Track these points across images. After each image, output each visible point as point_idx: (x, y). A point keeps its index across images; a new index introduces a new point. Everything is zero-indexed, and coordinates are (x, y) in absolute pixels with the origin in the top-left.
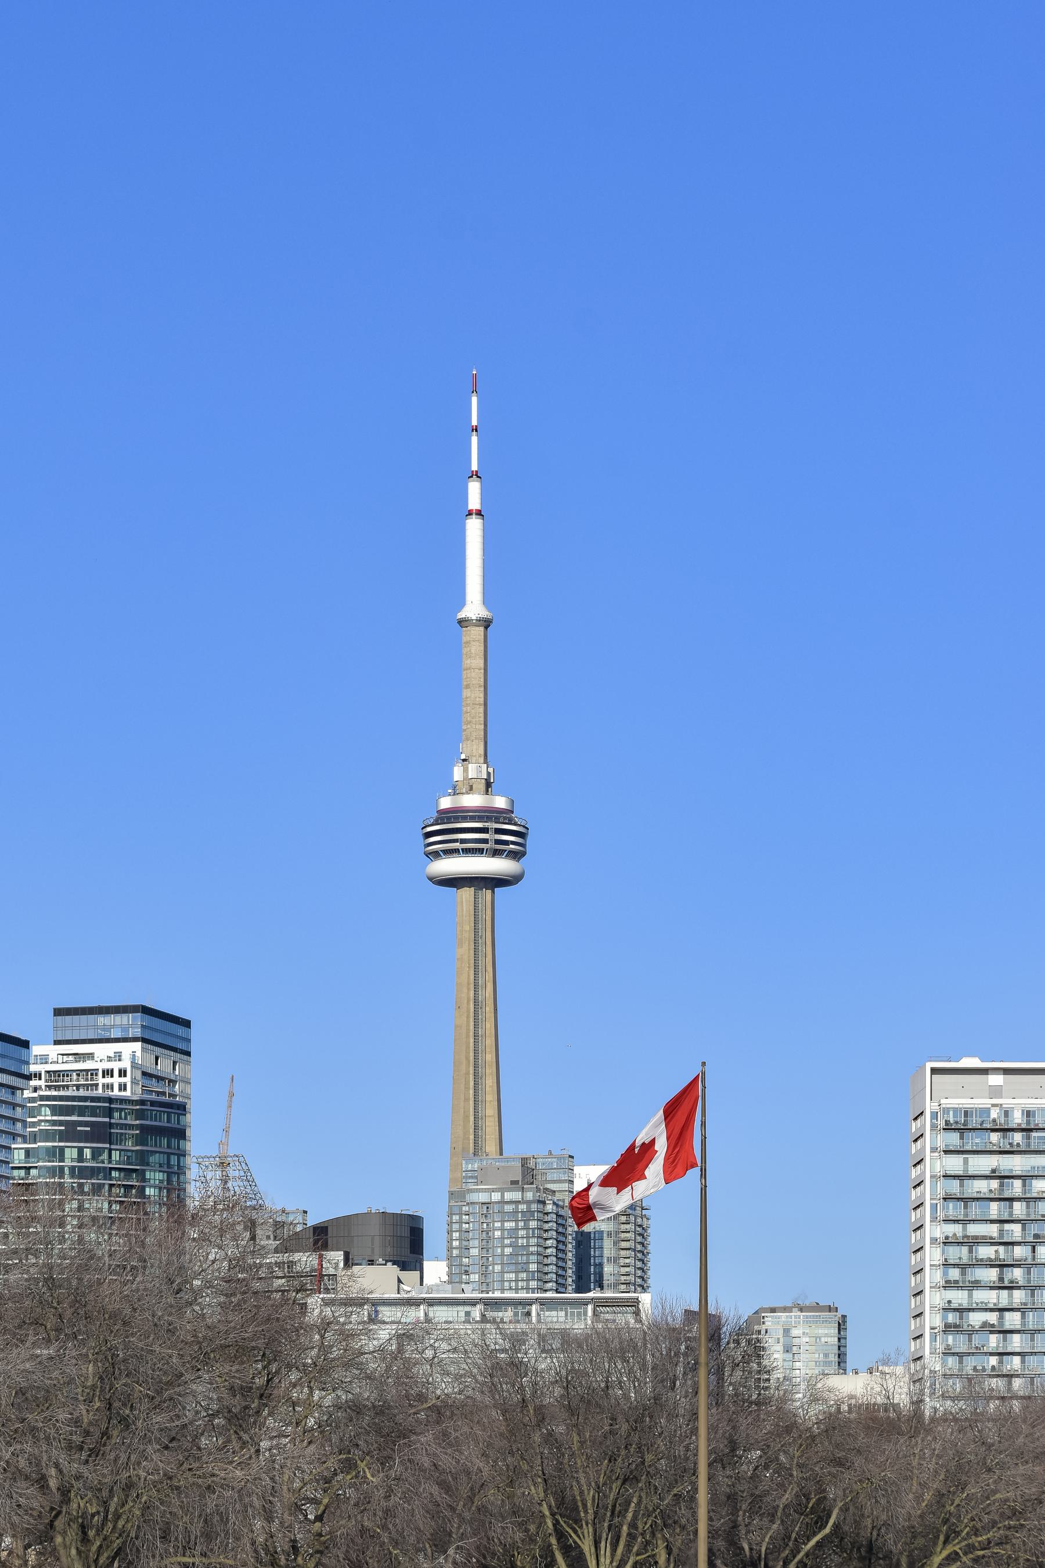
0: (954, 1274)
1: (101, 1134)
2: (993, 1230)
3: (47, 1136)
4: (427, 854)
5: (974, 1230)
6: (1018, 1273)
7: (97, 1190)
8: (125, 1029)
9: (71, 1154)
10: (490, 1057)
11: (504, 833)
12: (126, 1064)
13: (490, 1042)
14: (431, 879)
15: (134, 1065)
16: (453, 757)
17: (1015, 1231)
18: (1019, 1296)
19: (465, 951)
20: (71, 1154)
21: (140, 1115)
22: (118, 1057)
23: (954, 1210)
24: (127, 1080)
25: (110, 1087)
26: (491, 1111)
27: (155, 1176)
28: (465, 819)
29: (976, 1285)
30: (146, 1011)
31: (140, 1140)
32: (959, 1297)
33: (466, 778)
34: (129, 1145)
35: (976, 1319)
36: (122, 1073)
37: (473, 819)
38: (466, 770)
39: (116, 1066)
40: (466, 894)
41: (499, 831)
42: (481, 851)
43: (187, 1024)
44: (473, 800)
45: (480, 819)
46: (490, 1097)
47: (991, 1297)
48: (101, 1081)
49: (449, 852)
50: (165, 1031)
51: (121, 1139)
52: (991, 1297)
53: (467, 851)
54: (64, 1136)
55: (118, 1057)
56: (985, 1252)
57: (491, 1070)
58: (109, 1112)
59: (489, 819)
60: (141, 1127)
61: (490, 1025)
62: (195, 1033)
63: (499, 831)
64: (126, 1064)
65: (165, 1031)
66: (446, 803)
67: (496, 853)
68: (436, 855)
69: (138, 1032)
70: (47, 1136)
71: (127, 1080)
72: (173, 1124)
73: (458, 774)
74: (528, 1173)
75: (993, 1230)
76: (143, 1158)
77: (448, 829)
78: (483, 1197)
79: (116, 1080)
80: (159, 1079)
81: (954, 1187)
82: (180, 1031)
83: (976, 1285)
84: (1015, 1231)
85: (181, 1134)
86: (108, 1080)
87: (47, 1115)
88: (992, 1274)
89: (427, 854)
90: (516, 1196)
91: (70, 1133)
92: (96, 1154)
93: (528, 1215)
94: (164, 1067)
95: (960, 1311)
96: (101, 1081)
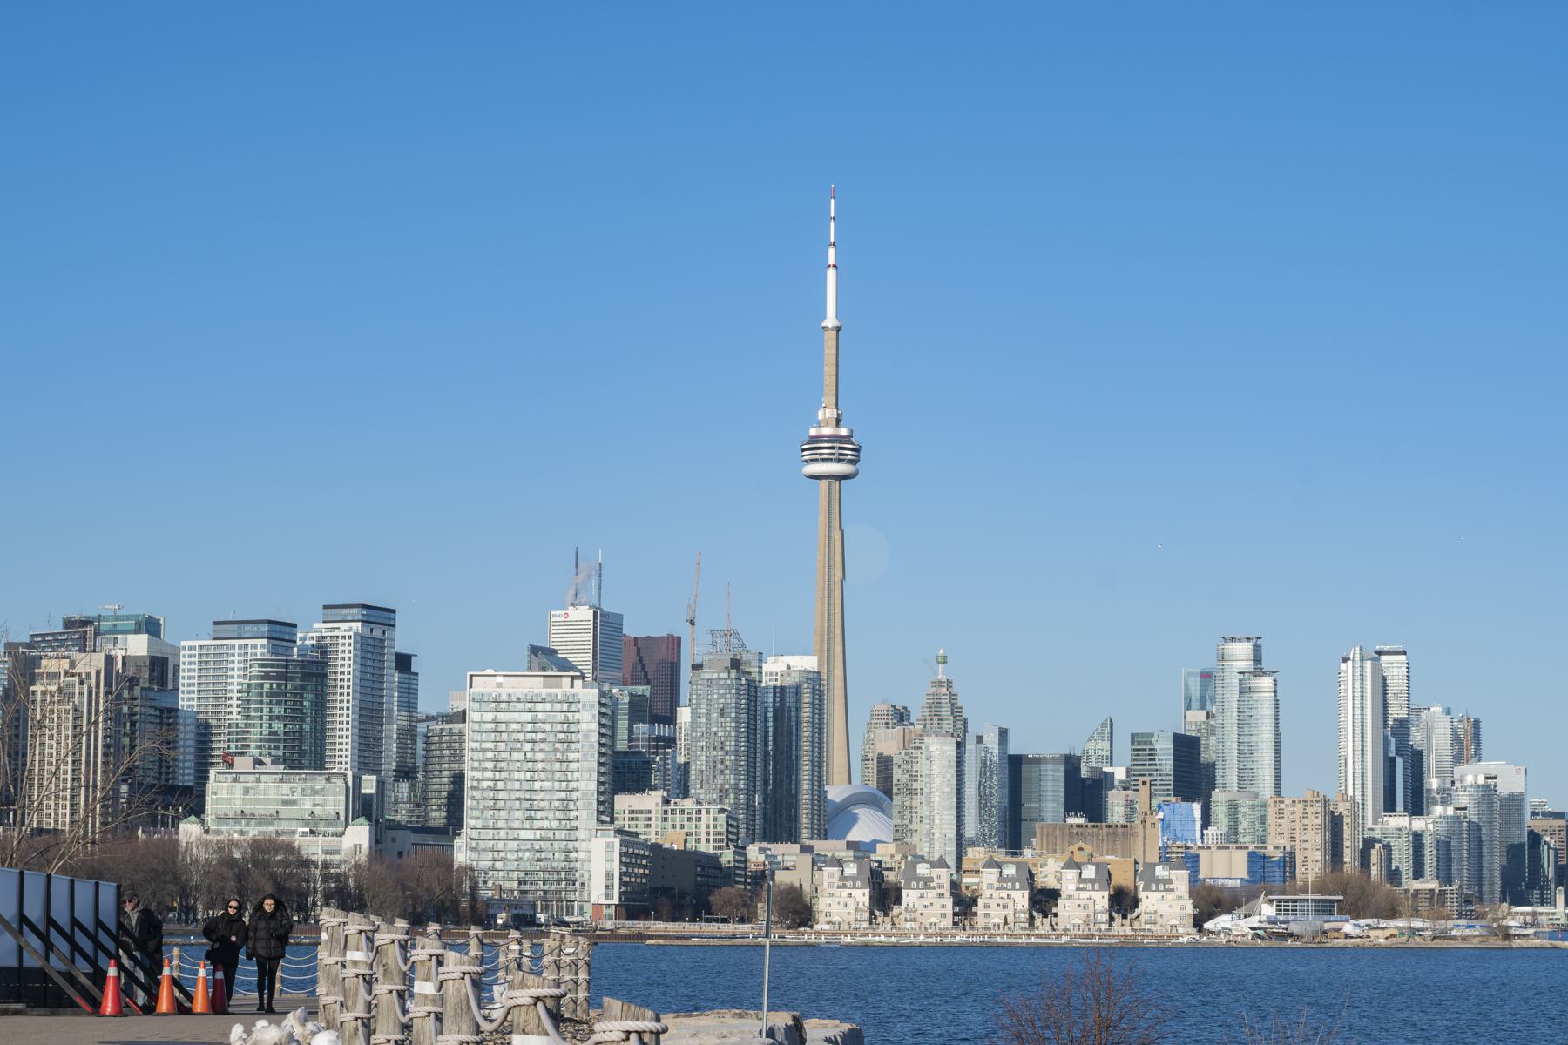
0: (476, 764)
1: (284, 676)
2: (491, 745)
3: (257, 677)
5: (485, 745)
6: (503, 765)
7: (279, 703)
9: (267, 686)
17: (502, 746)
18: (504, 775)
19: (822, 518)
20: (267, 686)
21: (303, 667)
23: (477, 737)
26: (838, 610)
27: (309, 696)
29: (485, 769)
30: (364, 606)
32: (477, 775)
35: (485, 784)
43: (394, 611)
46: (838, 602)
47: (489, 774)
50: (379, 617)
51: (292, 679)
52: (489, 774)
53: (823, 460)
54: (263, 678)
56: (490, 755)
58: (287, 666)
62: (398, 615)
65: (379, 617)
70: (257, 677)
74: (736, 664)
75: (491, 745)
76: (303, 688)
78: (708, 676)
81: (476, 727)
83: (485, 769)
84: (502, 746)
88: (490, 765)
90: (725, 675)
91: (266, 676)
92: (279, 686)
93: (731, 687)
94: (378, 632)
95: (478, 780)
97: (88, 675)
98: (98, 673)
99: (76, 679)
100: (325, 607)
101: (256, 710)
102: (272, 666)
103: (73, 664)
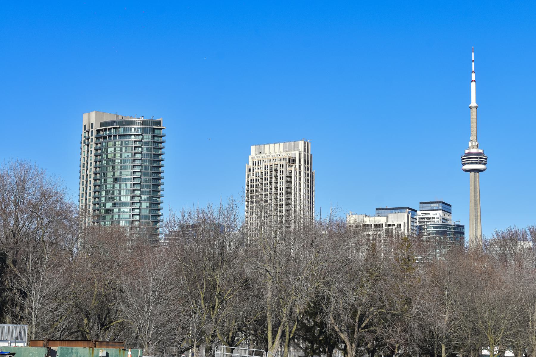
1: (445, 233)
4: (463, 164)
8: (438, 207)
10: (479, 214)
11: (481, 158)
12: (438, 216)
13: (478, 210)
14: (463, 170)
15: (440, 216)
16: (469, 140)
21: (454, 228)
22: (436, 214)
24: (439, 220)
25: (434, 222)
28: (472, 155)
30: (443, 203)
31: (454, 235)
33: (472, 145)
34: (451, 236)
36: (437, 218)
37: (474, 155)
38: (472, 143)
39: (436, 216)
40: (472, 174)
41: (480, 158)
42: (476, 163)
43: (450, 206)
44: (474, 151)
45: (476, 155)
48: (432, 220)
49: (468, 163)
53: (472, 163)
55: (436, 214)
57: (479, 217)
58: (447, 228)
59: (478, 155)
60: (454, 232)
61: (478, 206)
62: (453, 208)
63: (480, 158)
64: (438, 216)
66: (467, 151)
67: (480, 163)
68: (465, 164)
69: (441, 208)
70: (432, 234)
71: (439, 220)
72: (462, 231)
73: (470, 144)
77: (468, 158)
79: (436, 220)
80: (445, 219)
82: (449, 207)
85: (463, 233)
86: (434, 220)
87: (432, 228)
89: (463, 164)
91: (438, 233)
94: (446, 217)
96: (432, 220)
97: (399, 225)
98: (404, 224)
99: (394, 227)
100: (421, 203)
101: (433, 251)
102: (440, 227)
103: (387, 221)
